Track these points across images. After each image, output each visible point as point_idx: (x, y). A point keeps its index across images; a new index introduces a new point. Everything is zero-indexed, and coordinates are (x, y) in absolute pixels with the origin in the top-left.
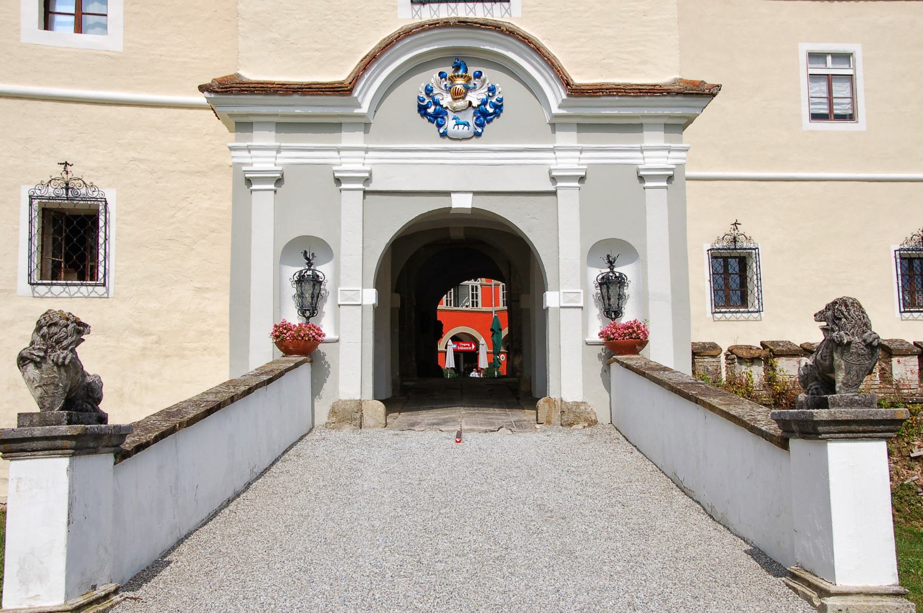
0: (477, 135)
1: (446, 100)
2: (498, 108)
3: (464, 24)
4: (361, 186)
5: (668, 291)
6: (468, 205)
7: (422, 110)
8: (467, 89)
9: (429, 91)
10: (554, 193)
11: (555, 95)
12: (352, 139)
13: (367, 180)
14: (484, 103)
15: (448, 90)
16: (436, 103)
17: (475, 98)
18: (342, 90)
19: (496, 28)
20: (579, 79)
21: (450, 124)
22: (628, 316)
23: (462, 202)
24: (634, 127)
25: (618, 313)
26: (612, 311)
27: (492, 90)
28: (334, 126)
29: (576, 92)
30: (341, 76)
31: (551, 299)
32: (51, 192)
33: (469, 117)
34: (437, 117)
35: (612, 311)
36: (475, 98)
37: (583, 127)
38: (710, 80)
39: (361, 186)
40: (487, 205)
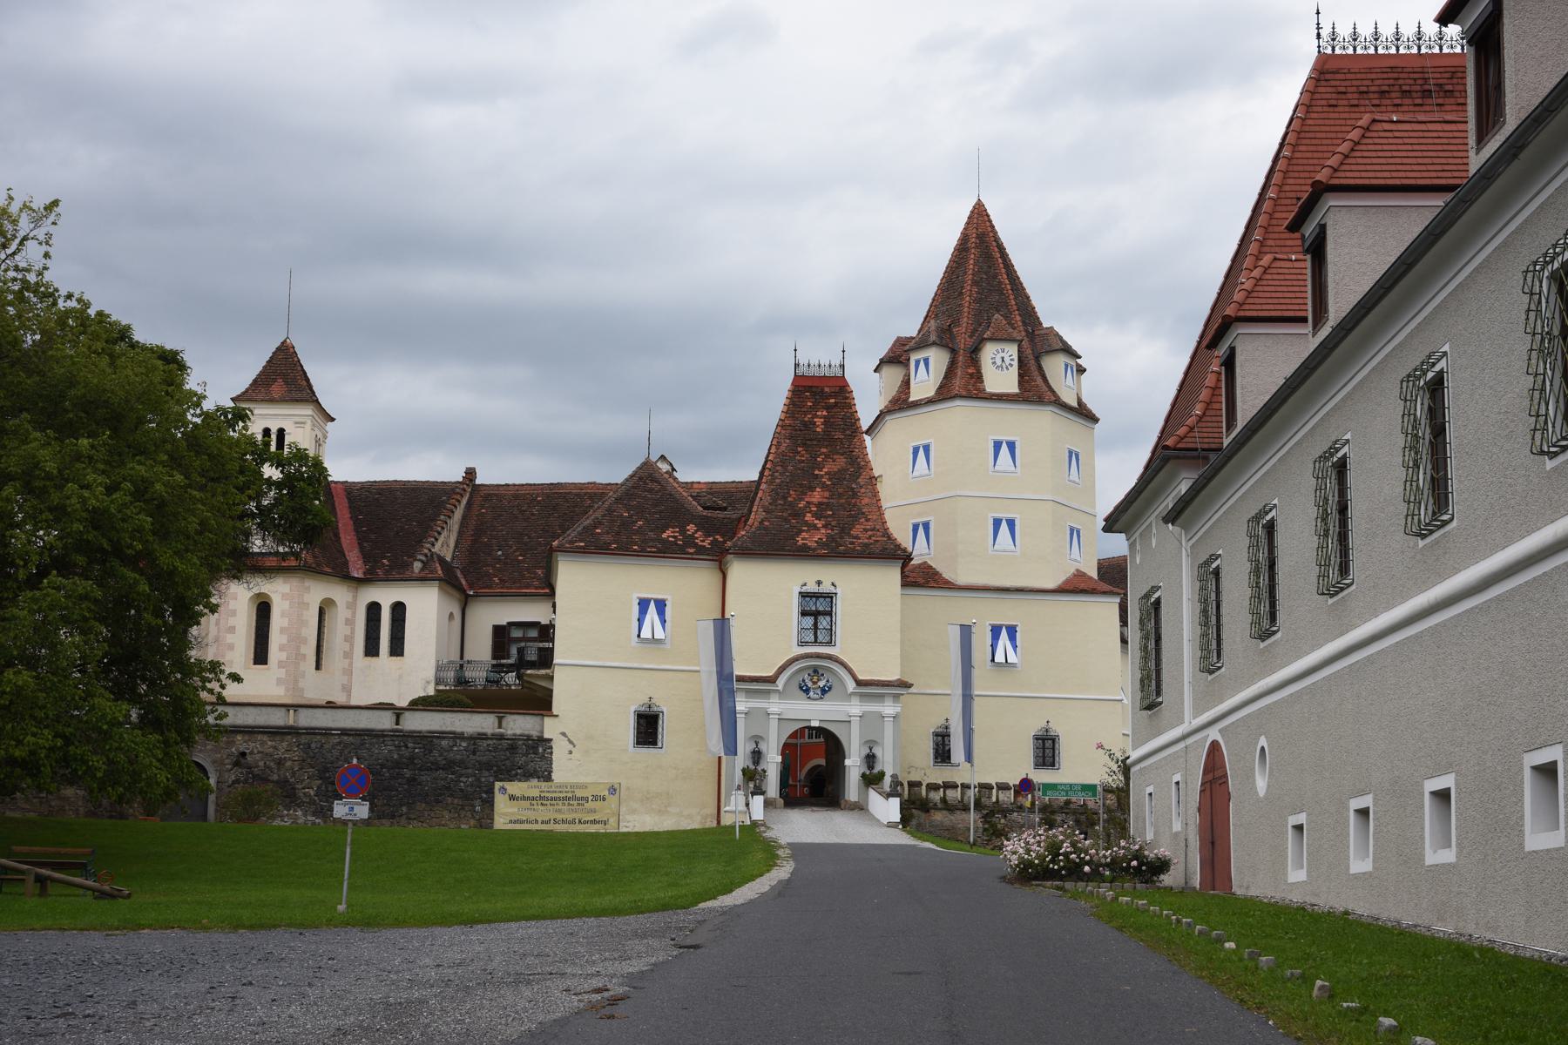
0: (822, 698)
1: (810, 684)
2: (830, 688)
3: (818, 656)
4: (777, 717)
5: (892, 761)
6: (817, 725)
7: (801, 688)
8: (818, 680)
9: (803, 681)
10: (850, 722)
11: (851, 685)
12: (774, 698)
13: (779, 715)
14: (824, 686)
15: (811, 680)
16: (807, 686)
17: (821, 684)
18: (771, 680)
19: (829, 657)
20: (861, 677)
21: (811, 694)
22: (875, 771)
23: (815, 724)
24: (881, 697)
25: (873, 768)
26: (871, 767)
27: (828, 681)
28: (768, 692)
29: (859, 683)
30: (770, 673)
31: (847, 762)
32: (643, 709)
33: (819, 692)
34: (807, 691)
35: (871, 767)
36: (821, 684)
37: (862, 695)
38: (910, 682)
39: (777, 717)
40: (824, 725)
